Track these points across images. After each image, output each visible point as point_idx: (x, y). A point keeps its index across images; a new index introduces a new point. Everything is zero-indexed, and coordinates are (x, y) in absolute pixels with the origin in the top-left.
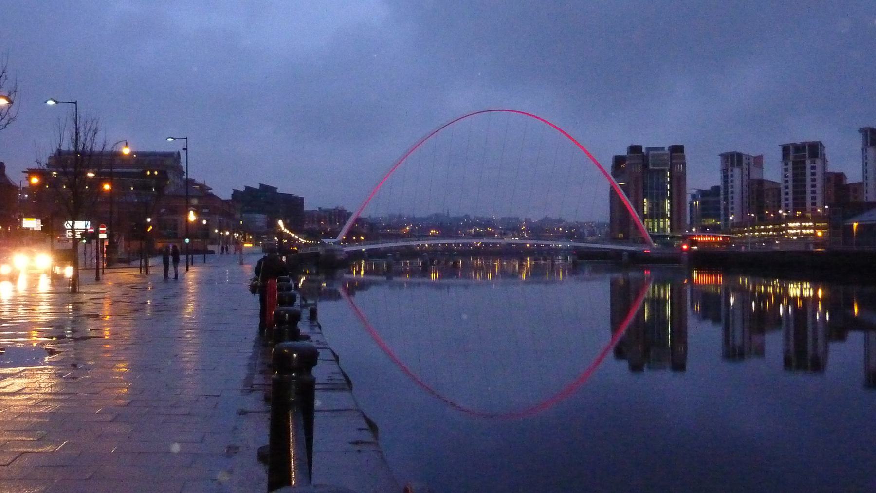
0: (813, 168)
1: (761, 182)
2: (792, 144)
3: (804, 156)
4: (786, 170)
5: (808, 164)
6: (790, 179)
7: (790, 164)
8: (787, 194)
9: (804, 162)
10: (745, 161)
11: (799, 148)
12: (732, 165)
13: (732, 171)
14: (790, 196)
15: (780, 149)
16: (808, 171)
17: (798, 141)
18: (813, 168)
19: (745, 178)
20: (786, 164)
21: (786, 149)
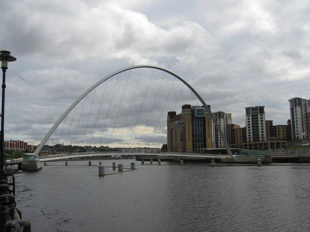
0: (262, 118)
1: (233, 125)
4: (249, 119)
5: (259, 115)
6: (251, 123)
7: (251, 116)
8: (249, 130)
10: (225, 116)
12: (220, 117)
13: (220, 120)
14: (251, 131)
15: (245, 110)
16: (259, 119)
18: (262, 118)
19: (226, 124)
20: (249, 116)
21: (248, 109)
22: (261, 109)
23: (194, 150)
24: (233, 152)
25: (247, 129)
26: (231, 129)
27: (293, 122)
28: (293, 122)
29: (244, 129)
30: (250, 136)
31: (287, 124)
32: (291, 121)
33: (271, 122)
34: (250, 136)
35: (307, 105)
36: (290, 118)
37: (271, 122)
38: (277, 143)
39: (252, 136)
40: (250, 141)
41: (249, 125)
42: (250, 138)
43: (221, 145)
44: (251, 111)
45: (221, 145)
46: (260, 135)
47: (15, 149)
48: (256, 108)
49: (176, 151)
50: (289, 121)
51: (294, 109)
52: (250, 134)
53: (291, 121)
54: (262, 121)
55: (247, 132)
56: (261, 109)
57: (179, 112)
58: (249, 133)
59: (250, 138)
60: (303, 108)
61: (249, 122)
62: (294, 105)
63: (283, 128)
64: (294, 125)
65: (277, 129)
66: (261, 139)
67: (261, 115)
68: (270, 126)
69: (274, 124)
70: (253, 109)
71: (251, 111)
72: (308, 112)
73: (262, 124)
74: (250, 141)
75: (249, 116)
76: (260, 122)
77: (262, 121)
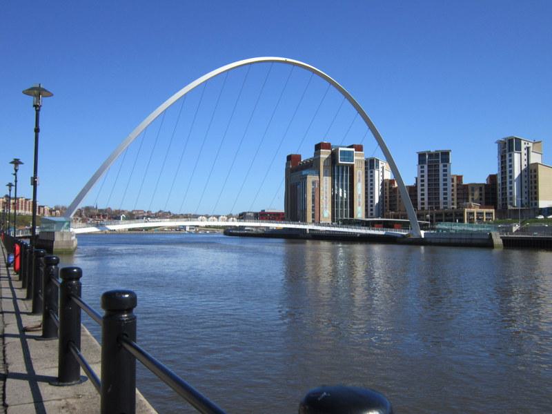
0: (445, 171)
2: (427, 152)
4: (422, 172)
5: (441, 165)
9: (438, 165)
10: (380, 166)
11: (434, 155)
13: (372, 172)
14: (426, 192)
15: (417, 155)
16: (441, 173)
17: (433, 150)
18: (445, 171)
19: (381, 178)
20: (422, 167)
21: (422, 156)
22: (445, 155)
23: (333, 220)
24: (423, 227)
25: (419, 188)
26: (390, 188)
27: (504, 178)
28: (504, 178)
29: (413, 190)
30: (423, 199)
31: (486, 182)
32: (499, 177)
33: (460, 178)
34: (423, 199)
35: (531, 150)
36: (495, 170)
37: (460, 178)
38: (477, 213)
39: (426, 199)
40: (423, 209)
41: (422, 181)
42: (423, 204)
43: (372, 214)
44: (427, 156)
45: (372, 214)
47: (12, 211)
49: (304, 220)
50: (492, 178)
51: (507, 155)
52: (423, 195)
53: (499, 177)
55: (419, 192)
56: (445, 155)
57: (307, 154)
58: (423, 195)
60: (523, 154)
61: (422, 176)
62: (507, 149)
63: (481, 189)
64: (504, 183)
65: (470, 189)
66: (442, 207)
67: (445, 166)
68: (457, 185)
69: (465, 182)
70: (431, 155)
71: (427, 156)
72: (532, 161)
73: (445, 180)
74: (423, 209)
76: (441, 177)
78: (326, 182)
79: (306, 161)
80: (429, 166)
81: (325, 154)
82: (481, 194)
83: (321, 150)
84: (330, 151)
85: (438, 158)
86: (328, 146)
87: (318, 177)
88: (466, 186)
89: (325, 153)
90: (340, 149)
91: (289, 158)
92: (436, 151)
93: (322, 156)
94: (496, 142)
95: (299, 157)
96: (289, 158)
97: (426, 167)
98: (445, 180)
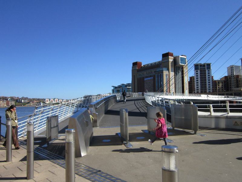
0: (209, 73)
3: (205, 69)
9: (205, 71)
14: (199, 84)
16: (207, 74)
18: (209, 73)
30: (197, 87)
39: (200, 88)
46: (207, 87)
48: (204, 65)
54: (209, 75)
56: (209, 65)
58: (197, 85)
59: (198, 90)
61: (197, 76)
70: (201, 65)
73: (209, 78)
75: (197, 71)
76: (207, 77)
77: (209, 75)
78: (172, 74)
79: (144, 66)
80: (200, 71)
81: (171, 59)
82: (222, 85)
83: (169, 57)
84: (173, 57)
85: (205, 67)
86: (172, 55)
87: (168, 72)
88: (215, 81)
89: (171, 58)
90: (180, 56)
91: (135, 64)
92: (204, 63)
93: (170, 60)
94: (240, 59)
95: (141, 63)
96: (135, 64)
97: (199, 71)
98: (209, 78)
